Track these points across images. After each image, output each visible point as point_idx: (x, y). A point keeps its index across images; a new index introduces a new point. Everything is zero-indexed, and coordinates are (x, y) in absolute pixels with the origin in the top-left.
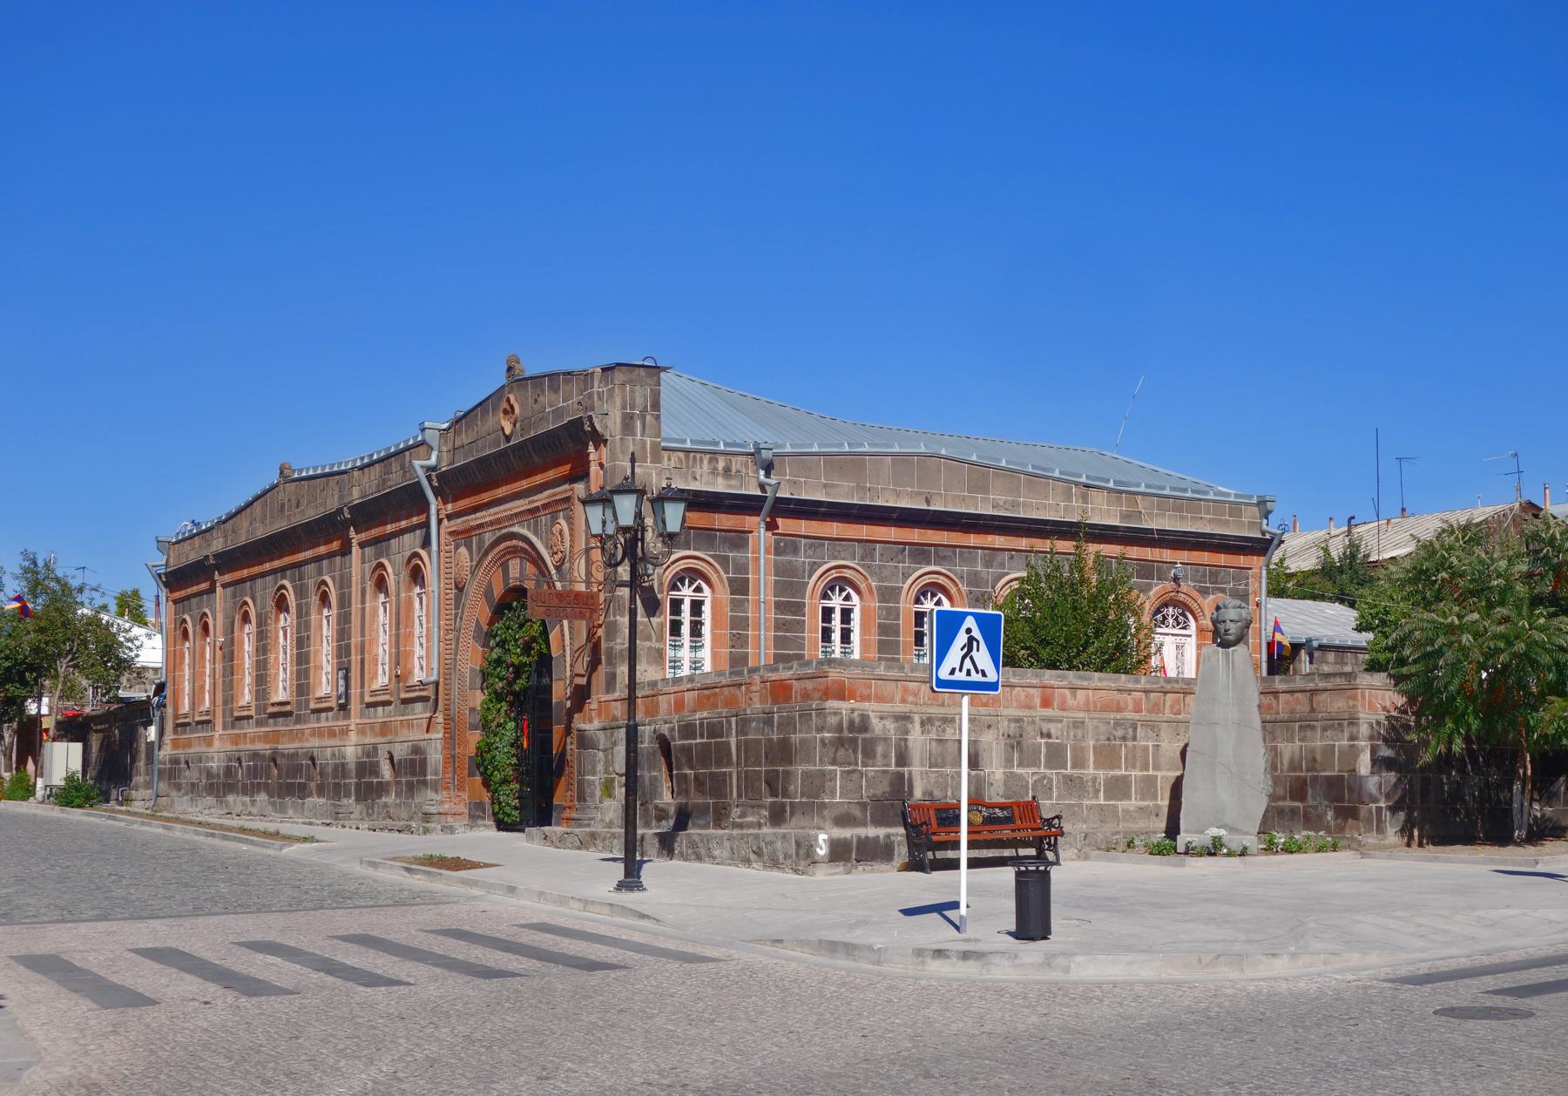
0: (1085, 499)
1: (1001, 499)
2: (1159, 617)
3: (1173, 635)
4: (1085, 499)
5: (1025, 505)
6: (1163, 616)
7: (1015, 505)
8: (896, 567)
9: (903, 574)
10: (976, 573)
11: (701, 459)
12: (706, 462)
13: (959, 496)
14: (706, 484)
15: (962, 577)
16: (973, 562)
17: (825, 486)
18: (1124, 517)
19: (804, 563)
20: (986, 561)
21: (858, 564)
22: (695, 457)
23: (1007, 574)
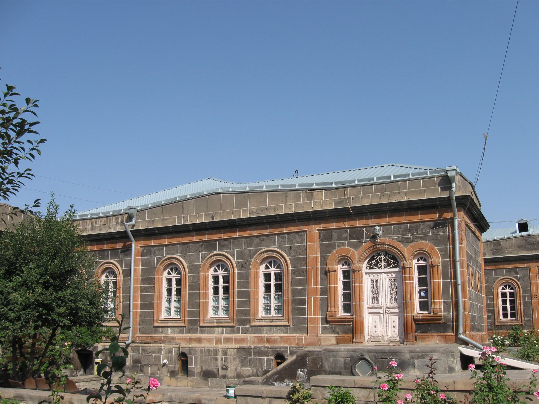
0: (309, 198)
1: (254, 208)
2: (373, 262)
3: (385, 273)
4: (309, 198)
5: (269, 209)
6: (377, 261)
7: (264, 210)
8: (198, 254)
9: (201, 257)
10: (242, 252)
11: (112, 220)
12: (114, 220)
13: (230, 212)
14: (114, 229)
15: (234, 255)
16: (241, 246)
17: (163, 220)
18: (336, 203)
19: (154, 258)
20: (248, 244)
21: (179, 256)
22: (110, 219)
23: (261, 249)
